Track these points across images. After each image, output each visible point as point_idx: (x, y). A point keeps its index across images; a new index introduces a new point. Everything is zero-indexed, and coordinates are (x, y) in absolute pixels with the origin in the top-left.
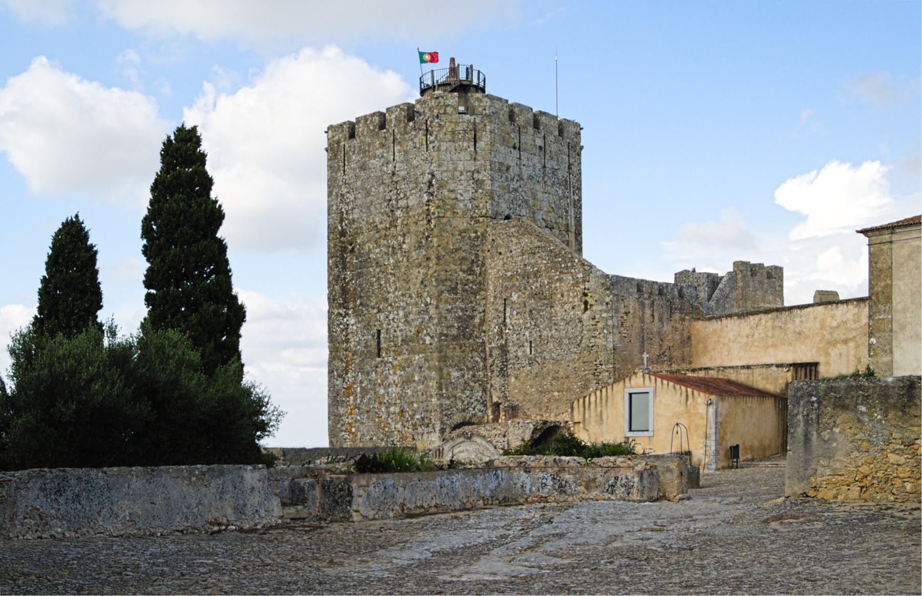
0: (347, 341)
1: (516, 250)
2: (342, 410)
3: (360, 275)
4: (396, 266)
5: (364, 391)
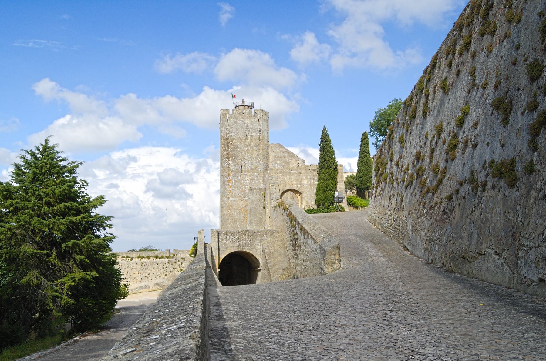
0: (229, 168)
1: (279, 151)
2: (226, 187)
3: (234, 151)
4: (248, 150)
5: (236, 182)
